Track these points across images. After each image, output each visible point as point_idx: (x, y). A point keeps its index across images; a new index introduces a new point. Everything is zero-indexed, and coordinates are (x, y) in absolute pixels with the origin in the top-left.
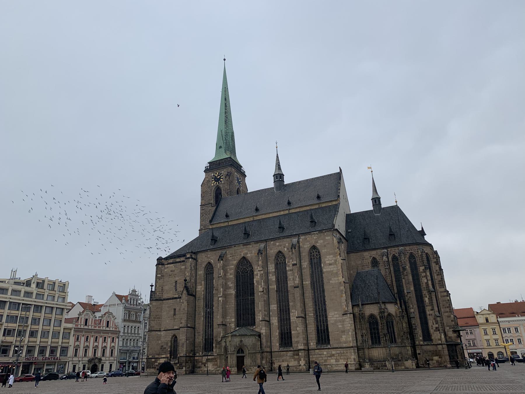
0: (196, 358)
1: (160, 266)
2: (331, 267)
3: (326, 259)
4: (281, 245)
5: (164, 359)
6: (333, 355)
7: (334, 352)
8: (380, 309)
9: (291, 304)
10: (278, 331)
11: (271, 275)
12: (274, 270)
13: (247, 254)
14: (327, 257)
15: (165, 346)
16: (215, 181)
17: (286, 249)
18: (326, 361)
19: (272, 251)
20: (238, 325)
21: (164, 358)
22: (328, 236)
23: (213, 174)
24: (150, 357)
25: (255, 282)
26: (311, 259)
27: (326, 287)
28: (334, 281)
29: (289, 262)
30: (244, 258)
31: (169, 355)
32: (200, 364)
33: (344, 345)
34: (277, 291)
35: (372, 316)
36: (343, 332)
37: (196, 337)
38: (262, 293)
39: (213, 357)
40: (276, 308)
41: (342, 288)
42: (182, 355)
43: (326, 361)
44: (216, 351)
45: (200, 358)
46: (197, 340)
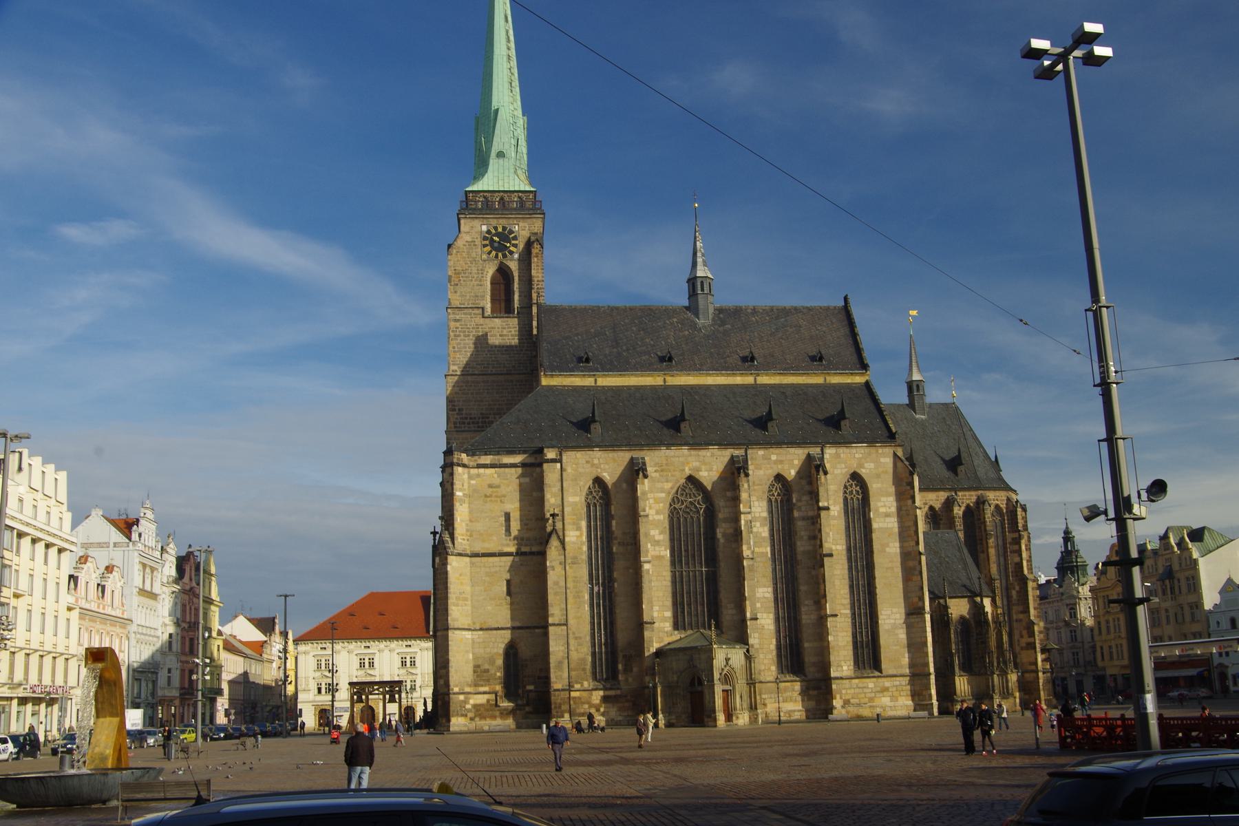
0: (573, 694)
1: (460, 469)
2: (888, 519)
3: (879, 504)
4: (781, 462)
5: (486, 696)
6: (887, 689)
10: (774, 641)
11: (758, 524)
12: (765, 514)
13: (698, 470)
14: (883, 499)
15: (486, 666)
16: (493, 248)
18: (871, 699)
19: (761, 472)
20: (676, 626)
21: (484, 693)
23: (484, 228)
24: (456, 690)
25: (719, 535)
26: (845, 499)
30: (691, 479)
31: (498, 688)
32: (586, 706)
37: (572, 647)
39: (618, 692)
42: (559, 686)
43: (871, 699)
44: (627, 680)
45: (585, 694)
46: (574, 655)
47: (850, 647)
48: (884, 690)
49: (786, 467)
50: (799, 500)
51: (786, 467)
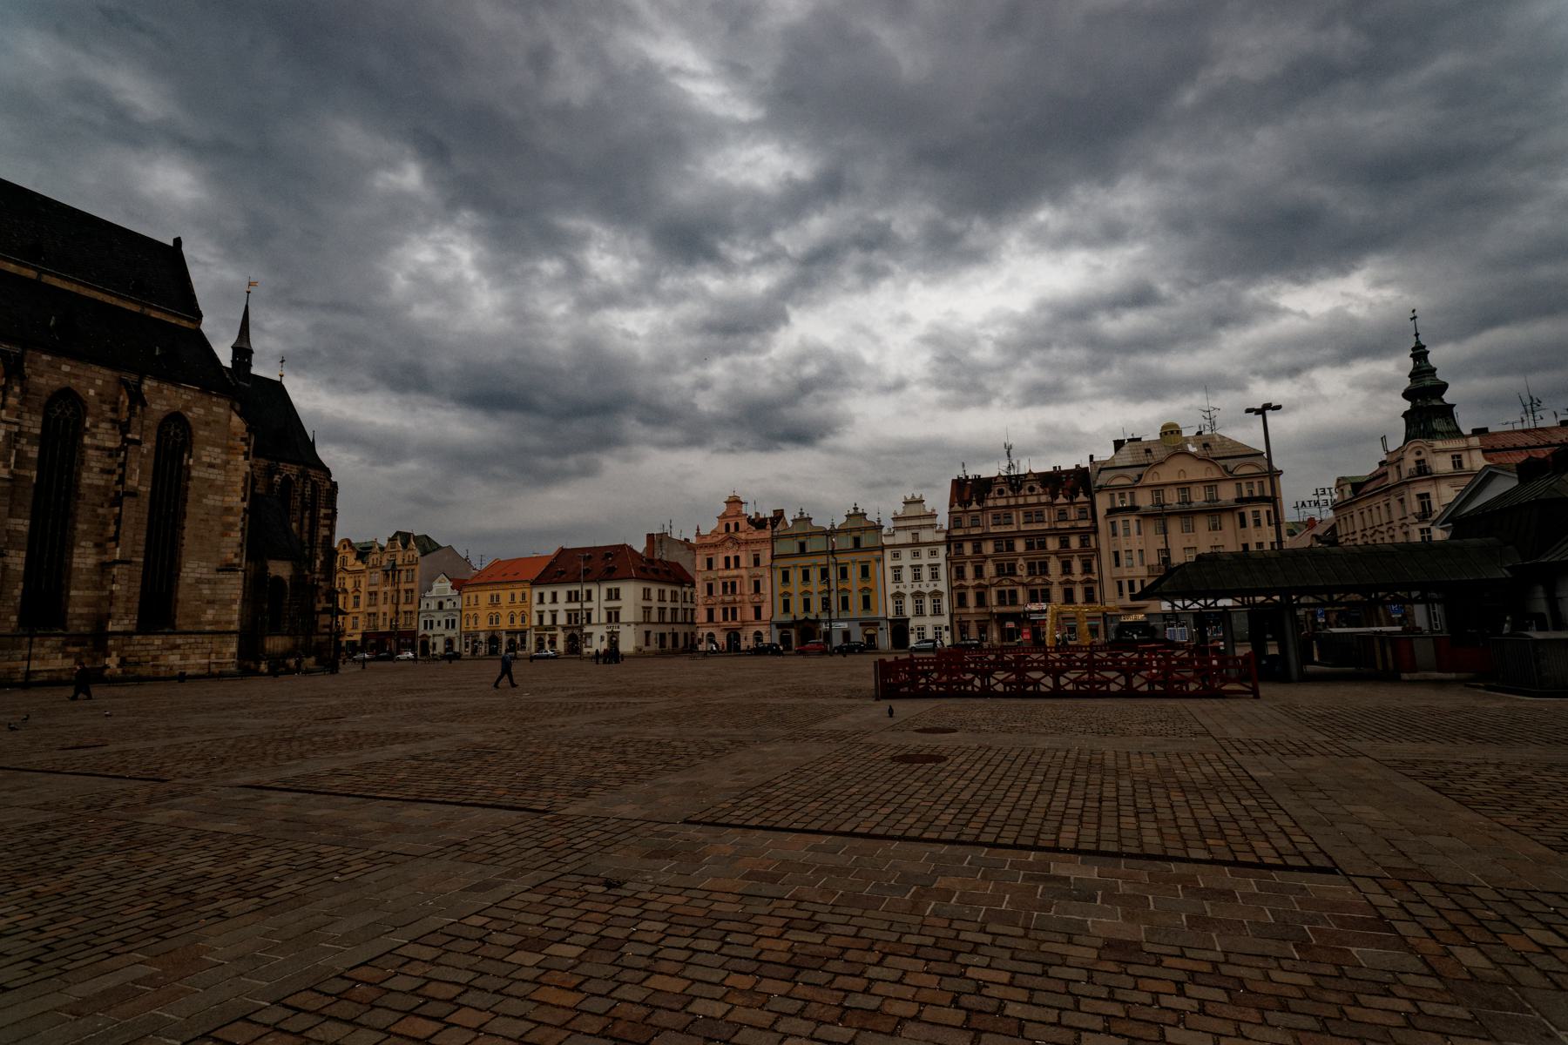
6: (178, 647)
7: (179, 641)
8: (297, 571)
9: (82, 527)
12: (38, 431)
17: (92, 392)
18: (155, 658)
19: (42, 381)
22: (218, 405)
27: (190, 509)
28: (212, 500)
29: (95, 426)
33: (208, 628)
34: (36, 486)
35: (278, 579)
36: (211, 602)
38: (7, 484)
40: (24, 529)
41: (236, 520)
43: (155, 658)
47: (137, 599)
48: (178, 647)
49: (83, 384)
50: (95, 426)
51: (83, 384)
